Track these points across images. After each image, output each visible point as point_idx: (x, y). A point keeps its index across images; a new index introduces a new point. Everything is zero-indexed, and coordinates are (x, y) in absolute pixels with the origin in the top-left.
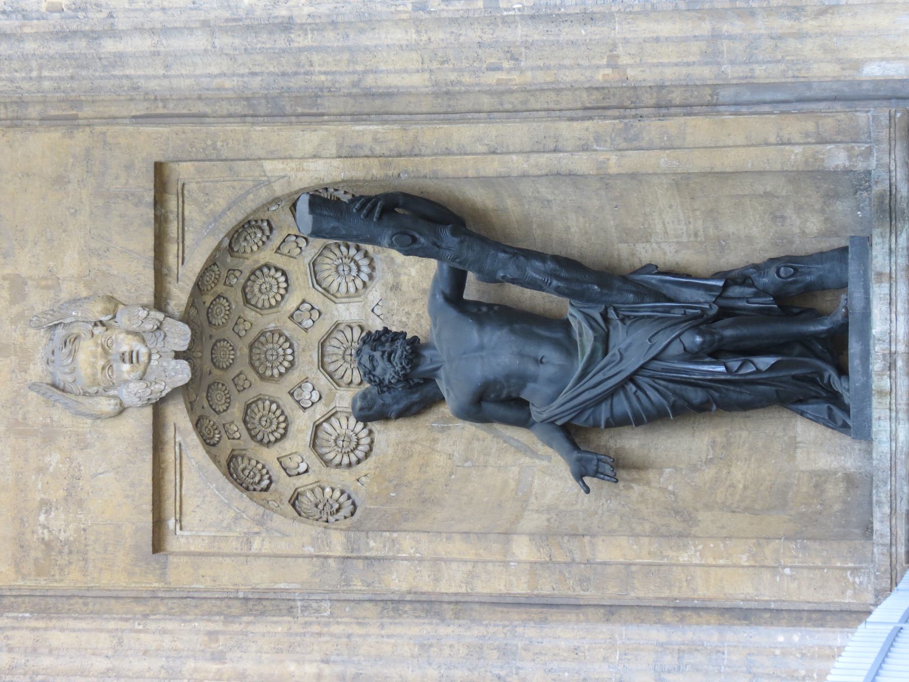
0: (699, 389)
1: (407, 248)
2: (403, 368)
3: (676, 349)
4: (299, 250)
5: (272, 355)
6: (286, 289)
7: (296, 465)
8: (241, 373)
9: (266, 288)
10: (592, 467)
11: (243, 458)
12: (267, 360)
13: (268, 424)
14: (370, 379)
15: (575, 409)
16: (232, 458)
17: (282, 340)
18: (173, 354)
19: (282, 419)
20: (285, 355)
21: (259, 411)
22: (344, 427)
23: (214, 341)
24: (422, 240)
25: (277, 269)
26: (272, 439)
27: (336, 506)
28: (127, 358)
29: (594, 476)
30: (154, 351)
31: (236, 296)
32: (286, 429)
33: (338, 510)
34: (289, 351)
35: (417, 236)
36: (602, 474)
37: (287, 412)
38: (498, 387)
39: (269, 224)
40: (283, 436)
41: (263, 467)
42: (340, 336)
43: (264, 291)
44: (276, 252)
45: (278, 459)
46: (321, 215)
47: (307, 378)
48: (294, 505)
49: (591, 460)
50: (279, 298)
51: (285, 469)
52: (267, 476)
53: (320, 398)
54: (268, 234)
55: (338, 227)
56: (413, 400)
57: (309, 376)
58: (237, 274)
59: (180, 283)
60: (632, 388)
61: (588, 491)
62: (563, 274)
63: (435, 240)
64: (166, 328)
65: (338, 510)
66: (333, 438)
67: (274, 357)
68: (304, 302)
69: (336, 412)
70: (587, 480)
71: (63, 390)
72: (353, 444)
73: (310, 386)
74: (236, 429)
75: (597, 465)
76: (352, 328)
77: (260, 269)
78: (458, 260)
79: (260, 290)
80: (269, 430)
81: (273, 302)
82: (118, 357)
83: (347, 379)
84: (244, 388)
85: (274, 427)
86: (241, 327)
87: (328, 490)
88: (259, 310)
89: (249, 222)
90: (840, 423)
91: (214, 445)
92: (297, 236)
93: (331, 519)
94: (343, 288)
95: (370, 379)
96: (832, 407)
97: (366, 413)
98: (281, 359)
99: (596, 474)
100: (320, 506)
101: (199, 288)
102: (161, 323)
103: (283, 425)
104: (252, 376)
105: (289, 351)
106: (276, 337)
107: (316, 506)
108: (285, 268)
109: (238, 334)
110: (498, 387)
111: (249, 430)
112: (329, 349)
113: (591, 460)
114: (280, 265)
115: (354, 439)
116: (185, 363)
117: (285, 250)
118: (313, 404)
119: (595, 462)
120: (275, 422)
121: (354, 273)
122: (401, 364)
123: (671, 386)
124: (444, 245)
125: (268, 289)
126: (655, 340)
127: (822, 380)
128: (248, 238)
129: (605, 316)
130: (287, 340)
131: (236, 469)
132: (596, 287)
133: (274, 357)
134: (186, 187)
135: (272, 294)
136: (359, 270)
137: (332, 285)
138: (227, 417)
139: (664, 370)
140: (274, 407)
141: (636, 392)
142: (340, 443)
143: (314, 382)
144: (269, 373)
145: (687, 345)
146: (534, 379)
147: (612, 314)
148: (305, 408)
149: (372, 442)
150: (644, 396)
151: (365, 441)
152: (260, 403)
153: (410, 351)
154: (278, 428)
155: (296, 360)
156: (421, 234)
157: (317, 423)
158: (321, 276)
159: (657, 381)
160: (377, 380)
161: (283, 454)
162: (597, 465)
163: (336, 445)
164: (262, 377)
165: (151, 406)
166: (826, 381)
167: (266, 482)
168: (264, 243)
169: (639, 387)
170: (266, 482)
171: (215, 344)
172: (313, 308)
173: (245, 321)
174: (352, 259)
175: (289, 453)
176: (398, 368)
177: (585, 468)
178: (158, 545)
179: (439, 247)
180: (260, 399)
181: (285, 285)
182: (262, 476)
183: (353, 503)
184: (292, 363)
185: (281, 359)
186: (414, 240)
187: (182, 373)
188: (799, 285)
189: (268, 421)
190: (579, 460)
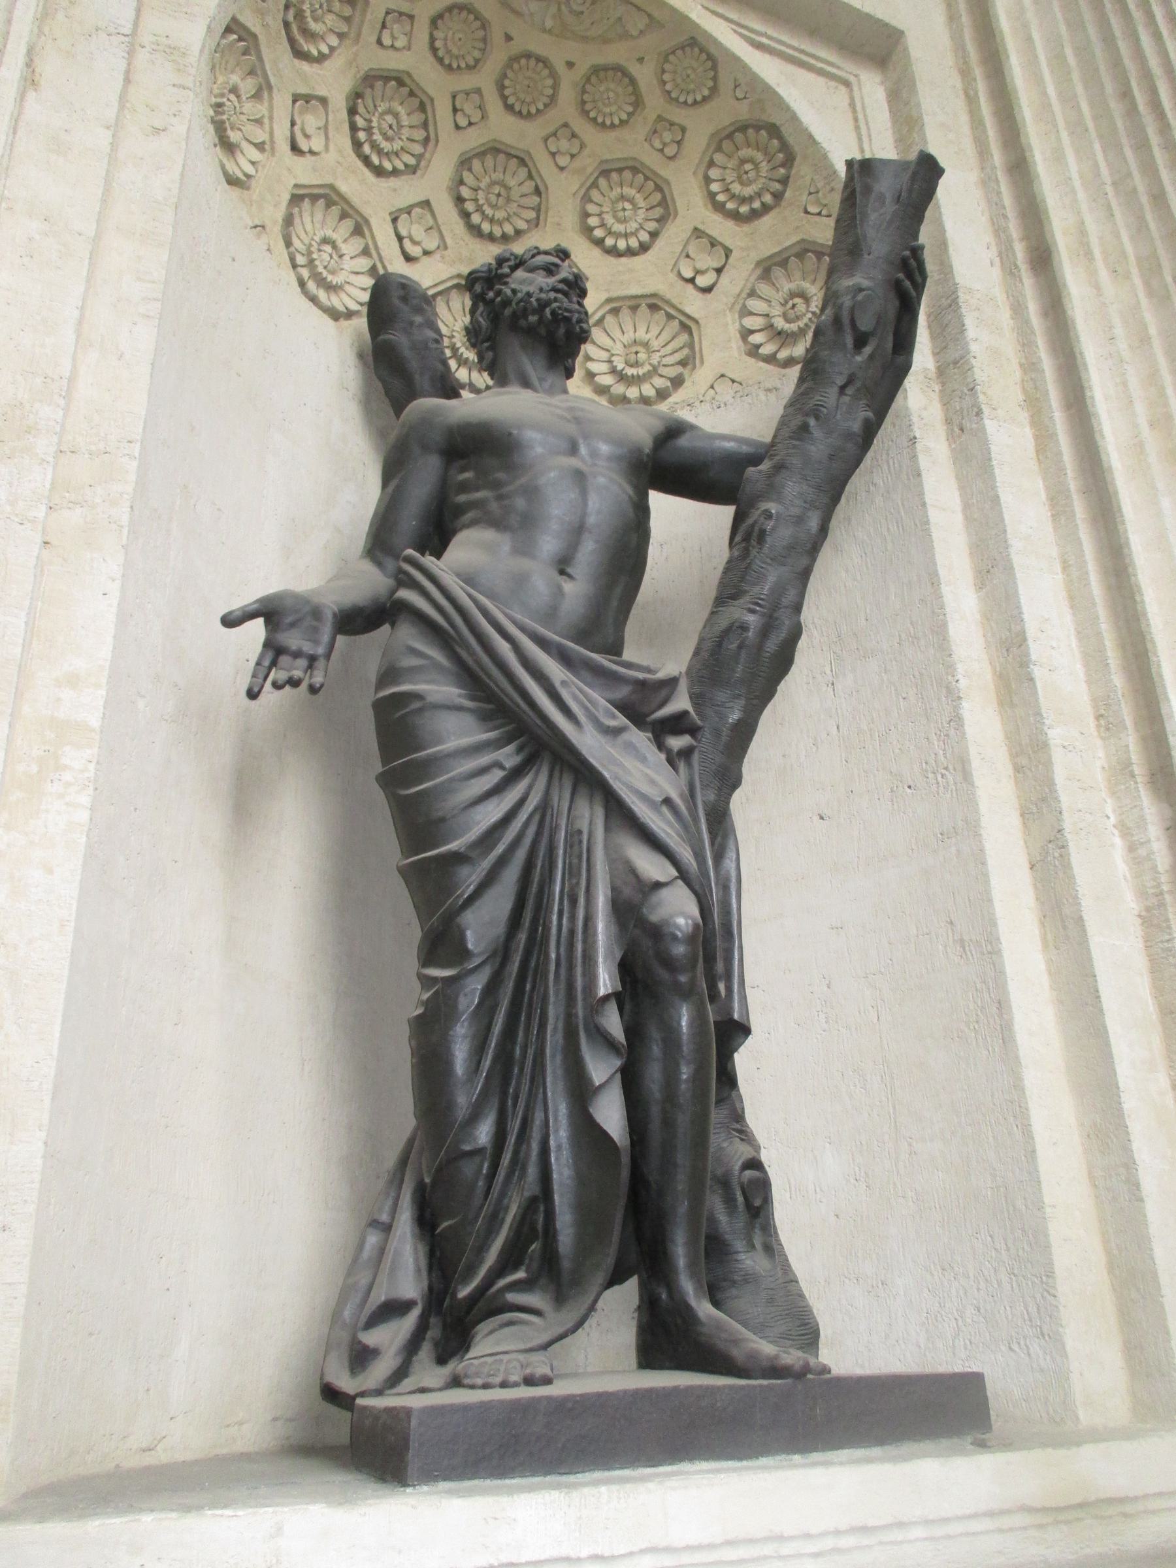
0: (500, 929)
1: (846, 320)
2: (543, 304)
3: (652, 866)
4: (688, 274)
5: (499, 195)
6: (613, 252)
7: (309, 131)
9: (624, 209)
10: (293, 640)
11: (348, 20)
13: (385, 126)
14: (508, 260)
15: (458, 621)
22: (354, 279)
23: (561, 68)
24: (859, 358)
25: (654, 235)
26: (360, 122)
29: (267, 644)
35: (868, 350)
36: (274, 663)
38: (501, 475)
39: (766, 209)
40: (357, 145)
43: (620, 206)
44: (696, 229)
45: (324, 101)
46: (914, 174)
47: (446, 248)
49: (316, 642)
50: (598, 233)
51: (307, 98)
55: (883, 204)
56: (417, 376)
57: (449, 252)
59: (700, 7)
60: (509, 756)
61: (229, 622)
62: (772, 645)
63: (858, 384)
66: (339, 243)
70: (256, 629)
72: (320, 269)
73: (431, 244)
74: (398, 44)
75: (297, 655)
77: (664, 203)
78: (812, 422)
79: (623, 198)
80: (374, 124)
81: (593, 221)
84: (455, 110)
85: (377, 137)
86: (564, 144)
87: (254, 154)
88: (583, 191)
90: (371, 1338)
92: (719, 271)
95: (508, 260)
96: (415, 1313)
97: (395, 294)
99: (274, 650)
100: (232, 97)
104: (474, 139)
109: (555, 134)
110: (501, 475)
113: (316, 642)
114: (660, 243)
115: (330, 278)
118: (400, 239)
119: (307, 648)
120: (386, 146)
122: (556, 300)
123: (521, 854)
124: (846, 399)
125: (621, 214)
126: (665, 809)
127: (514, 1286)
128: (748, 167)
129: (678, 724)
132: (734, 716)
133: (493, 198)
134: (843, 89)
135: (609, 220)
137: (604, 335)
139: (574, 835)
141: (502, 767)
142: (328, 248)
143: (437, 256)
144: (468, 177)
145: (664, 893)
146: (524, 549)
147: (677, 743)
150: (487, 787)
151: (322, 295)
153: (578, 329)
154: (375, 146)
155: (478, 240)
156: (871, 357)
159: (537, 818)
160: (506, 270)
162: (297, 655)
163: (325, 241)
164: (465, 163)
166: (513, 1297)
169: (515, 775)
173: (573, 156)
175: (331, 135)
176: (543, 296)
177: (293, 625)
179: (842, 389)
180: (427, 140)
186: (861, 341)
188: (722, 1218)
189: (390, 133)
190: (316, 613)
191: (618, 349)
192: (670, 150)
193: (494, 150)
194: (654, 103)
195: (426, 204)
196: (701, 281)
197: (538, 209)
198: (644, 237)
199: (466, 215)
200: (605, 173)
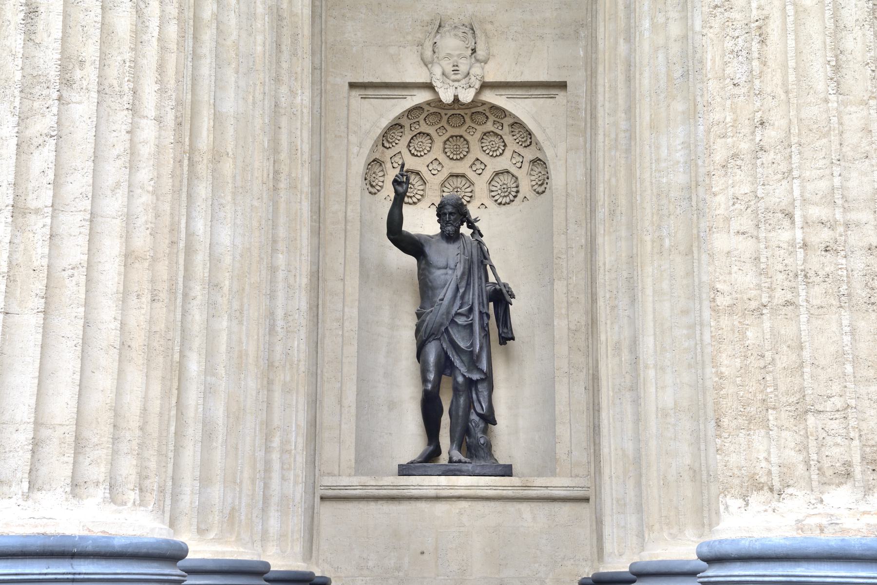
5: (456, 148)
8: (446, 131)
16: (402, 127)
17: (465, 153)
18: (456, 94)
19: (423, 154)
20: (457, 154)
21: (426, 141)
25: (503, 150)
27: (374, 184)
28: (456, 68)
30: (460, 84)
31: (489, 126)
32: (417, 156)
33: (372, 186)
34: (459, 157)
37: (425, 156)
40: (413, 155)
41: (396, 144)
48: (374, 161)
50: (487, 152)
52: (391, 146)
53: (434, 175)
54: (523, 145)
64: (471, 89)
65: (372, 186)
68: (486, 166)
69: (425, 184)
71: (437, 32)
76: (471, 192)
80: (416, 146)
82: (455, 64)
83: (445, 189)
87: (381, 179)
89: (530, 134)
91: (408, 116)
93: (367, 181)
94: (494, 189)
101: (494, 108)
102: (473, 87)
104: (445, 138)
105: (459, 157)
106: (467, 150)
107: (374, 173)
108: (505, 153)
111: (415, 136)
112: (459, 180)
116: (452, 99)
128: (521, 133)
130: (465, 156)
131: (394, 129)
138: (422, 122)
140: (429, 149)
148: (428, 166)
149: (410, 204)
152: (430, 141)
161: (403, 154)
165: (429, 81)
167: (387, 145)
168: (518, 143)
170: (387, 145)
171: (462, 116)
172: (483, 170)
178: (353, 86)
181: (494, 155)
182: (391, 143)
183: (375, 194)
184: (452, 159)
185: (455, 153)
187: (447, 97)
191: (499, 187)
192: (500, 128)
193: (452, 137)
194: (492, 118)
196: (519, 165)
197: (468, 148)
198: (501, 152)
199: (449, 156)
200: (485, 134)
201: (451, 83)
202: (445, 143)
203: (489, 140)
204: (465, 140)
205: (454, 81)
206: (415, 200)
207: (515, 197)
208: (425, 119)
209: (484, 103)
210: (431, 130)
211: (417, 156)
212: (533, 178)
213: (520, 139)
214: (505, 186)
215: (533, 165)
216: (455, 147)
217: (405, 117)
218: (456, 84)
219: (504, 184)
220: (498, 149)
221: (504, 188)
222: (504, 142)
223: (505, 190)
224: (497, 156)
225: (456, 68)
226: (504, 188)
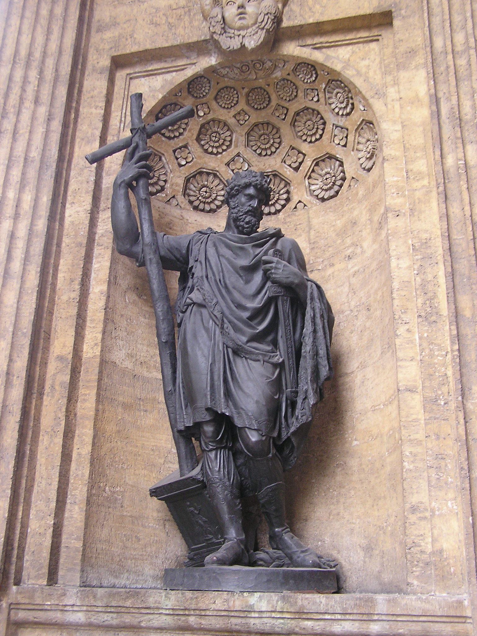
6: (311, 142)
12: (261, 135)
25: (323, 130)
28: (240, 10)
42: (282, 186)
58: (315, 99)
67: (263, 141)
98: (263, 147)
103: (215, 151)
117: (336, 131)
121: (325, 187)
125: (308, 128)
136: (326, 190)
157: (218, 174)
158: (322, 164)
174: (334, 184)
181: (313, 139)
193: (256, 125)
195: (238, 155)
196: (343, 143)
201: (236, 33)
202: (248, 134)
203: (303, 121)
204: (274, 127)
205: (239, 29)
206: (213, 206)
207: (341, 186)
208: (216, 99)
209: (285, 60)
210: (227, 116)
211: (212, 153)
212: (360, 155)
213: (340, 106)
214: (328, 176)
215: (359, 135)
216: (262, 138)
217: (185, 93)
218: (242, 33)
219: (328, 173)
220: (317, 132)
221: (326, 179)
222: (322, 118)
223: (329, 181)
224: (317, 140)
225: (240, 10)
226: (326, 179)
